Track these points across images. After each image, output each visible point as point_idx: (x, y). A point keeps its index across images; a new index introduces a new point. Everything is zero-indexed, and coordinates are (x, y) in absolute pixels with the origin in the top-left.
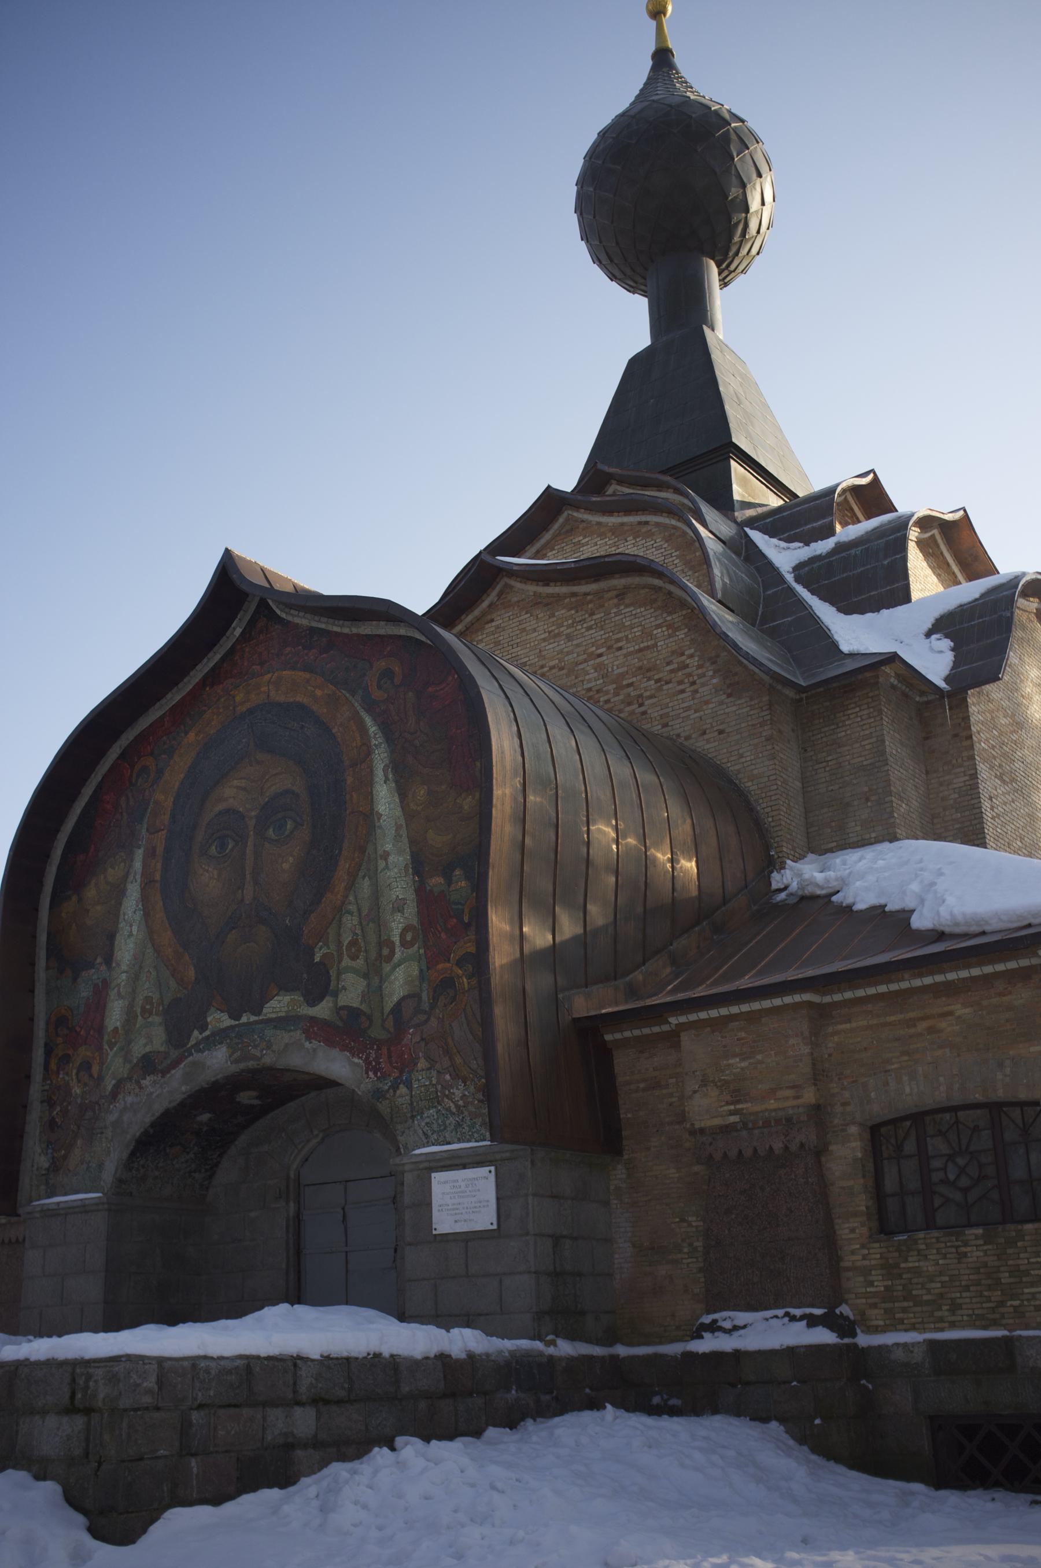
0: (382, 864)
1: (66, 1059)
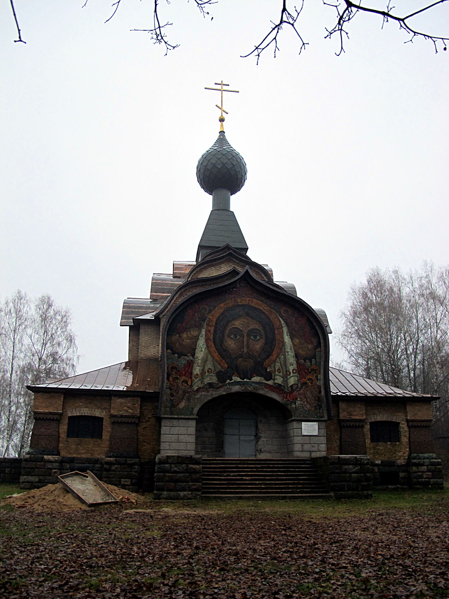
0: (287, 354)
1: (177, 378)
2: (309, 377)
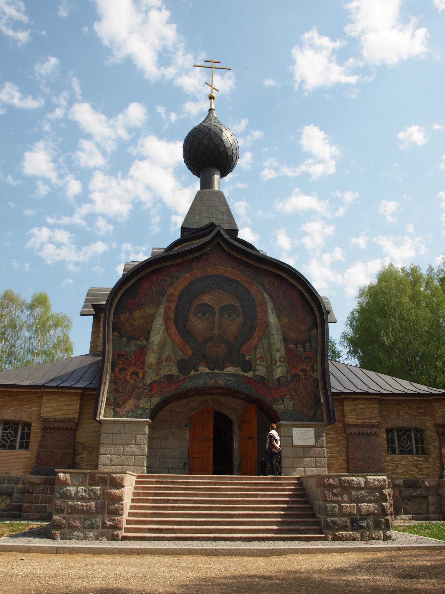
0: (272, 337)
1: (125, 369)
2: (301, 367)
